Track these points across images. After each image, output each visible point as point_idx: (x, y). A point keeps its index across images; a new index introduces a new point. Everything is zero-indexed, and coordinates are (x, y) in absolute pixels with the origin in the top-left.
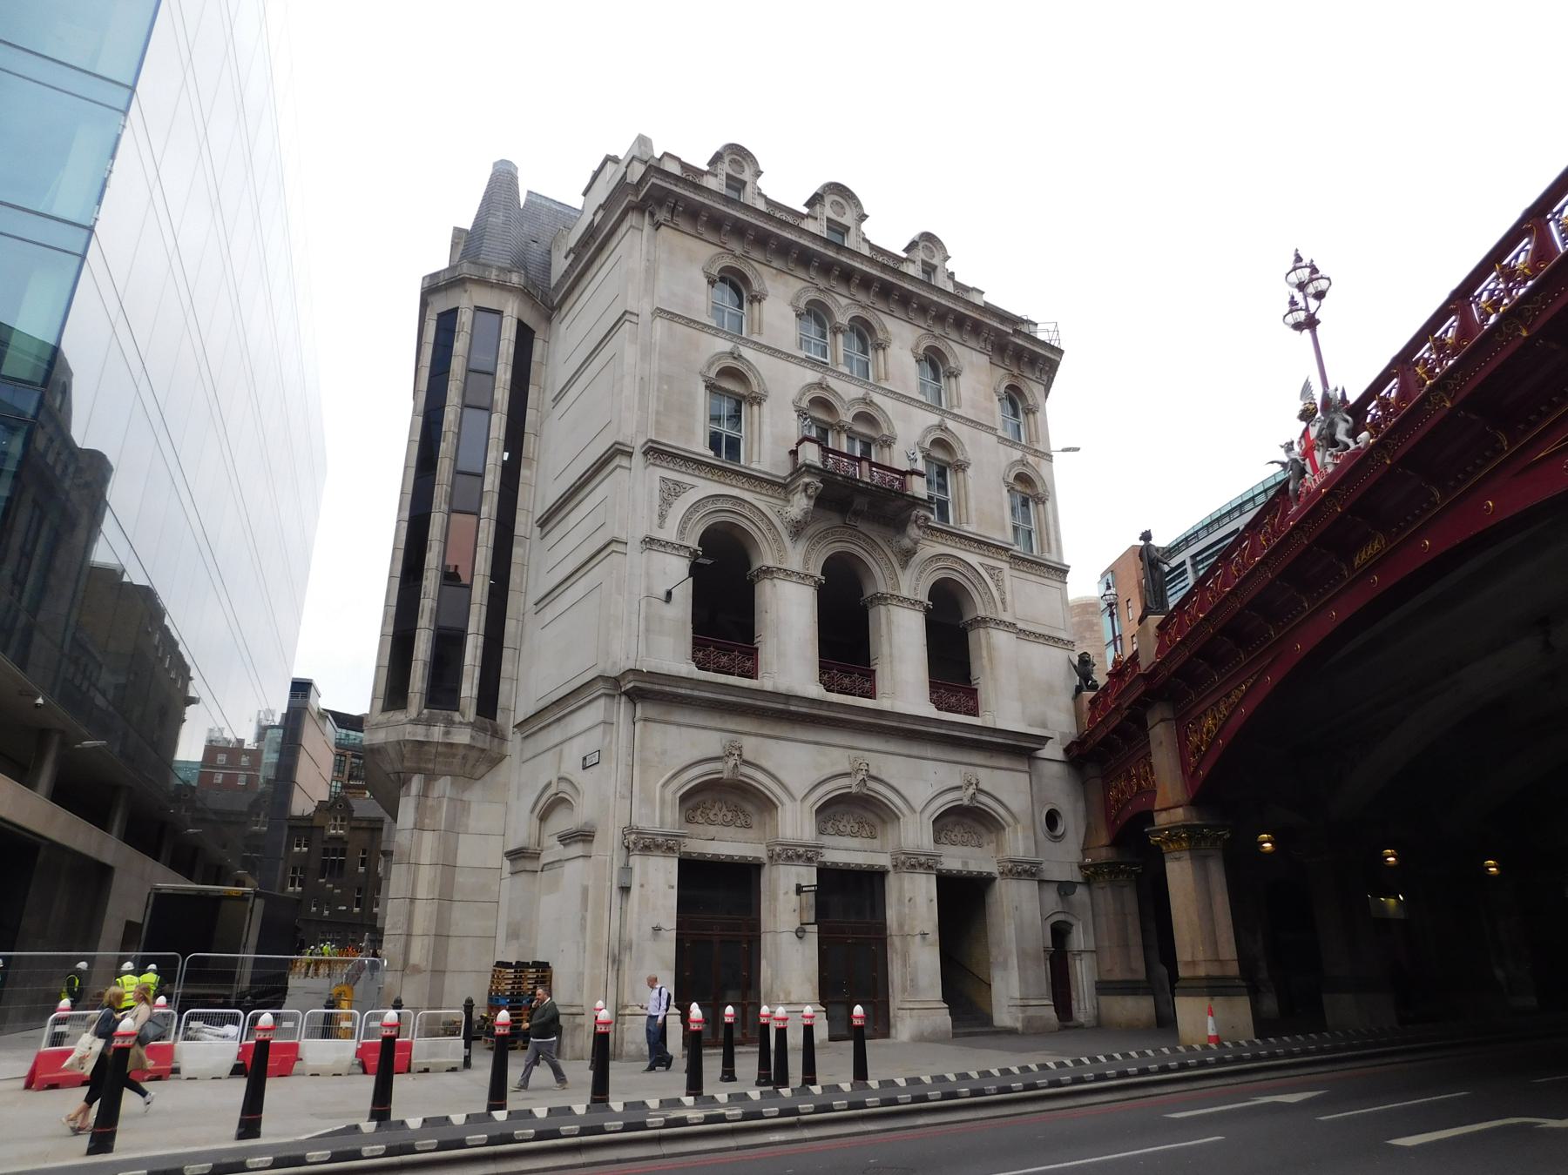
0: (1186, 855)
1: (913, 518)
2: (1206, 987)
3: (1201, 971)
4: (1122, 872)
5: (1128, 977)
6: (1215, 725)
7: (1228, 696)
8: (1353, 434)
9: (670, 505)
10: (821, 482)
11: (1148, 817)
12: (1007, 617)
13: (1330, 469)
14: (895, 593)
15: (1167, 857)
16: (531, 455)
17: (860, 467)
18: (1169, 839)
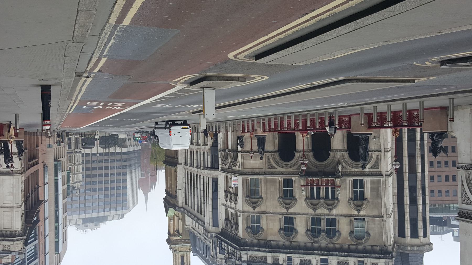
9: (375, 162)
16: (395, 196)
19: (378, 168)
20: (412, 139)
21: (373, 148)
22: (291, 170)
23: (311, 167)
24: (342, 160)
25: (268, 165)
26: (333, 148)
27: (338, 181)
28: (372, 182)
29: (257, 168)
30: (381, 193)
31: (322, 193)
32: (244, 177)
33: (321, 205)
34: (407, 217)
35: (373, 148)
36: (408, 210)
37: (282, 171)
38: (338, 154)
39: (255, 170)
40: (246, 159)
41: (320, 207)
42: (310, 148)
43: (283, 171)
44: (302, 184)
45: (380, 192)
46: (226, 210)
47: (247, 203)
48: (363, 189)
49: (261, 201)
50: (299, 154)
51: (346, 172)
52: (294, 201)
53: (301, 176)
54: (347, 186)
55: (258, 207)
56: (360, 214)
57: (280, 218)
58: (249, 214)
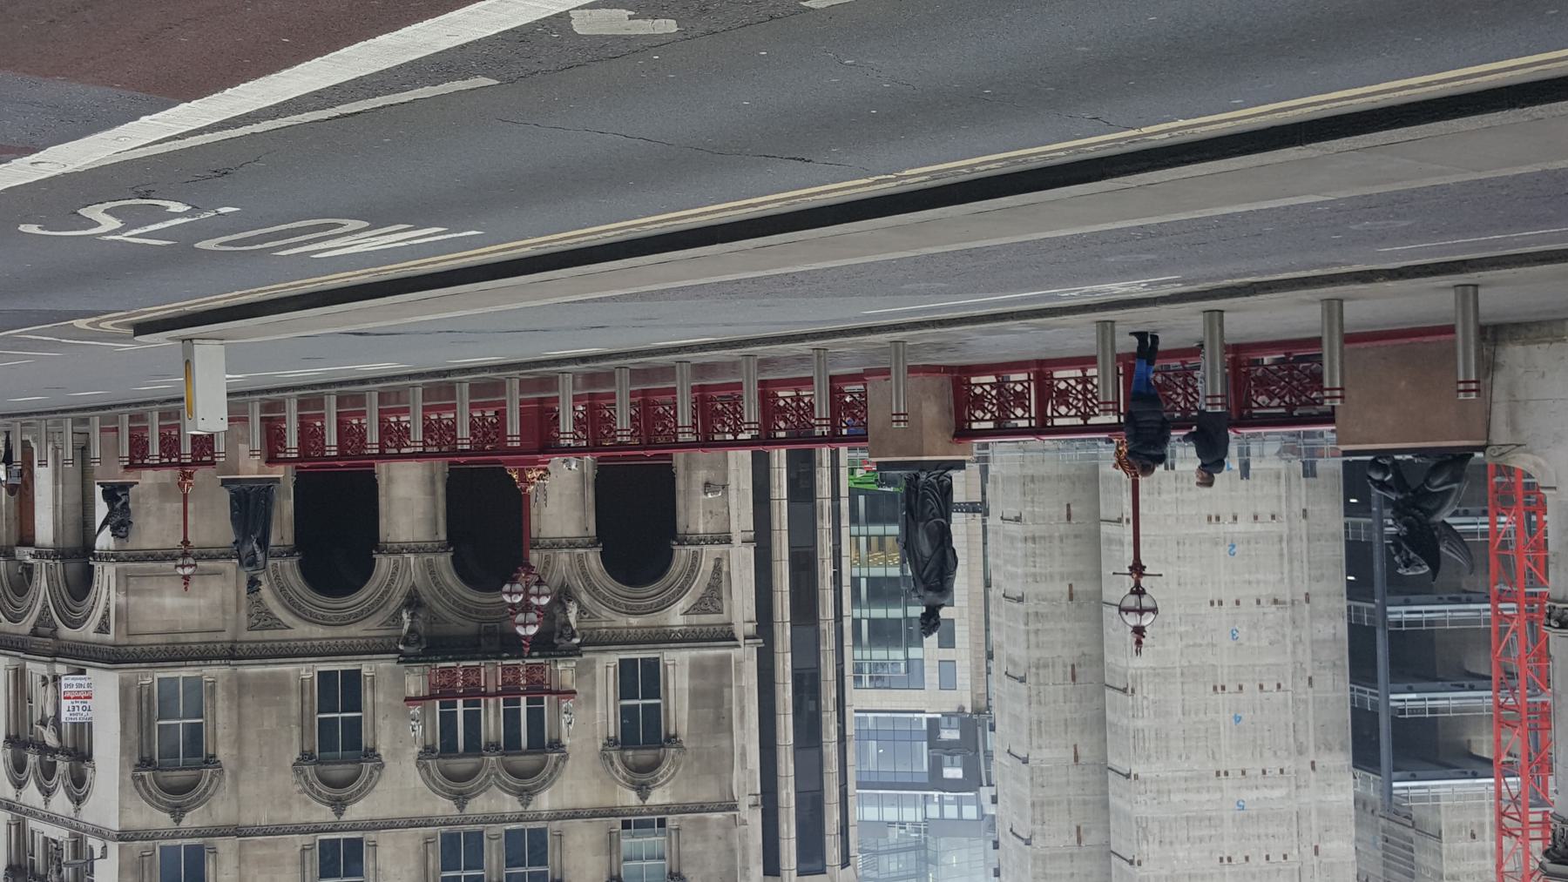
1: (424, 640)
10: (557, 645)
14: (428, 557)
17: (497, 686)
19: (720, 611)
20: (802, 490)
21: (701, 532)
22: (356, 630)
23: (449, 615)
24: (578, 584)
25: (250, 616)
26: (540, 530)
27: (564, 671)
28: (698, 669)
29: (196, 628)
30: (730, 710)
31: (492, 724)
32: (127, 674)
33: (488, 777)
34: (788, 794)
35: (701, 532)
36: (791, 766)
37: (314, 636)
38: (563, 556)
39: (183, 638)
40: (138, 592)
41: (484, 788)
42: (443, 536)
43: (320, 636)
44: (412, 692)
45: (726, 707)
46: (13, 827)
47: (145, 793)
48: (659, 697)
49: (211, 781)
50: (396, 562)
51: (595, 634)
52: (367, 767)
53: (406, 659)
54: (598, 690)
55: (198, 806)
56: (647, 802)
57: (303, 850)
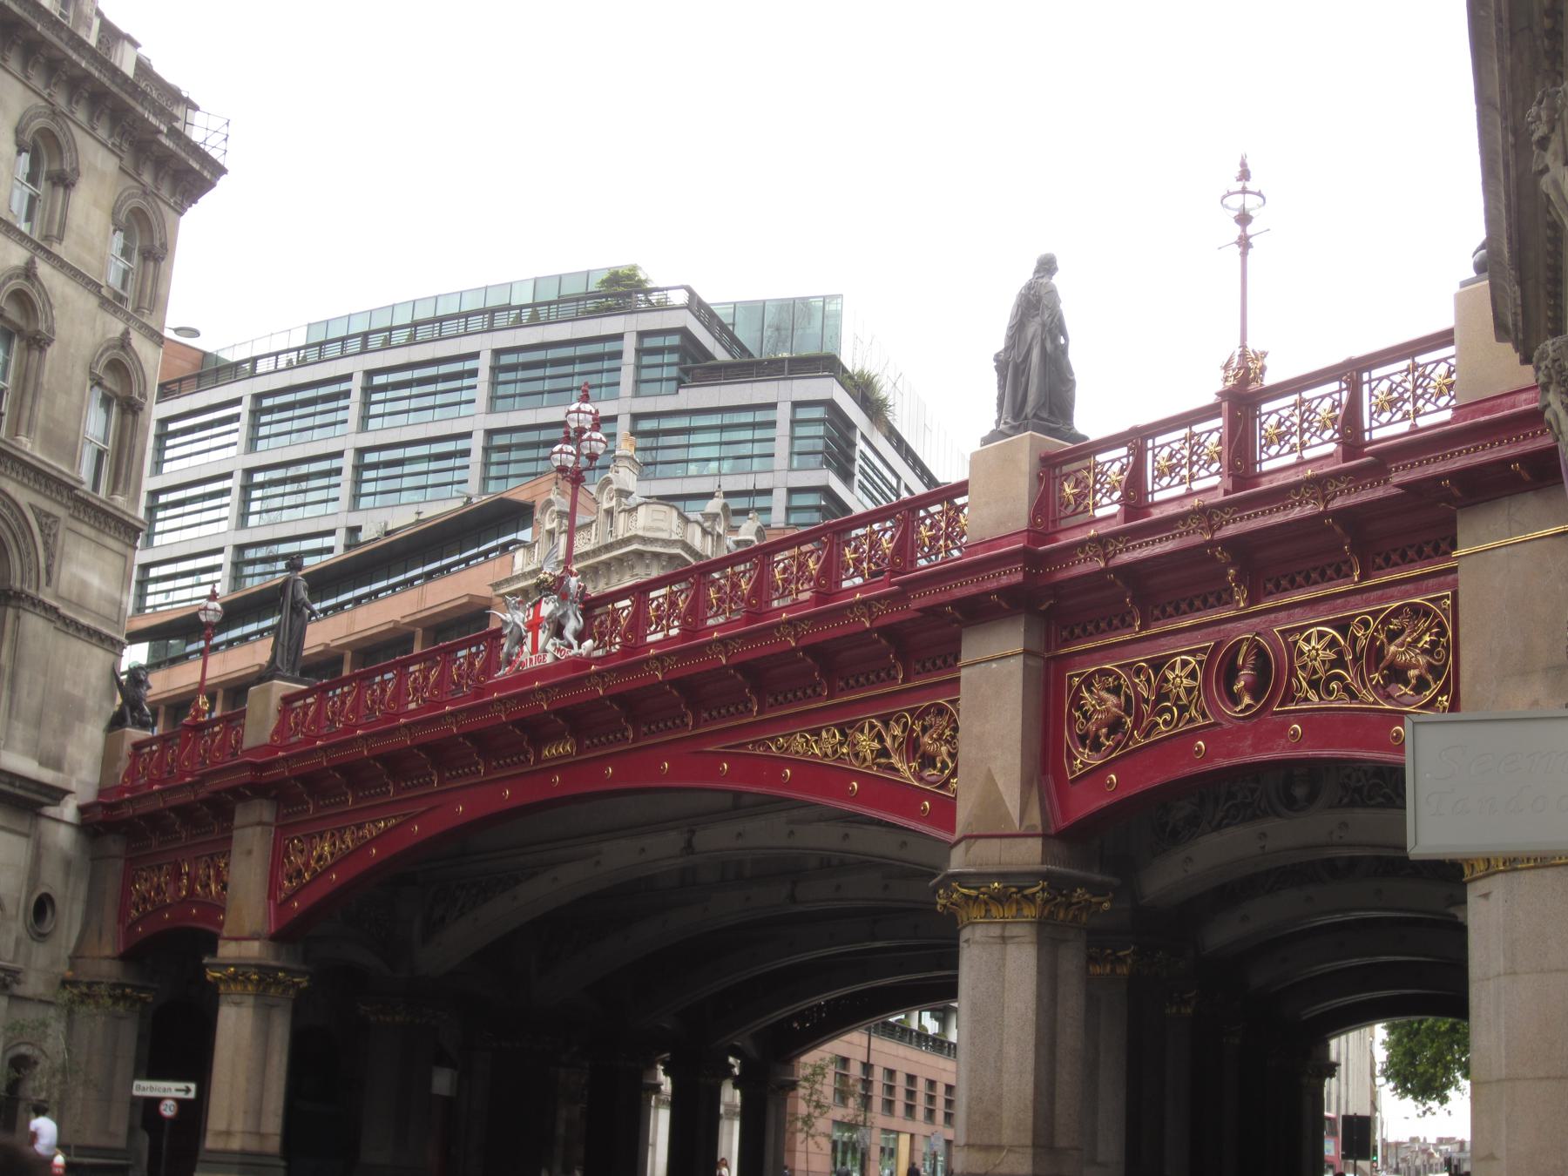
0: (250, 1000)
2: (240, 1164)
3: (235, 1144)
4: (124, 997)
5: (103, 1141)
6: (332, 854)
7: (360, 827)
8: (581, 637)
11: (210, 942)
12: (47, 596)
13: (549, 659)
15: (222, 998)
18: (234, 978)
25: (55, 536)
29: (84, 541)
57: (60, 239)
58: (144, 321)
